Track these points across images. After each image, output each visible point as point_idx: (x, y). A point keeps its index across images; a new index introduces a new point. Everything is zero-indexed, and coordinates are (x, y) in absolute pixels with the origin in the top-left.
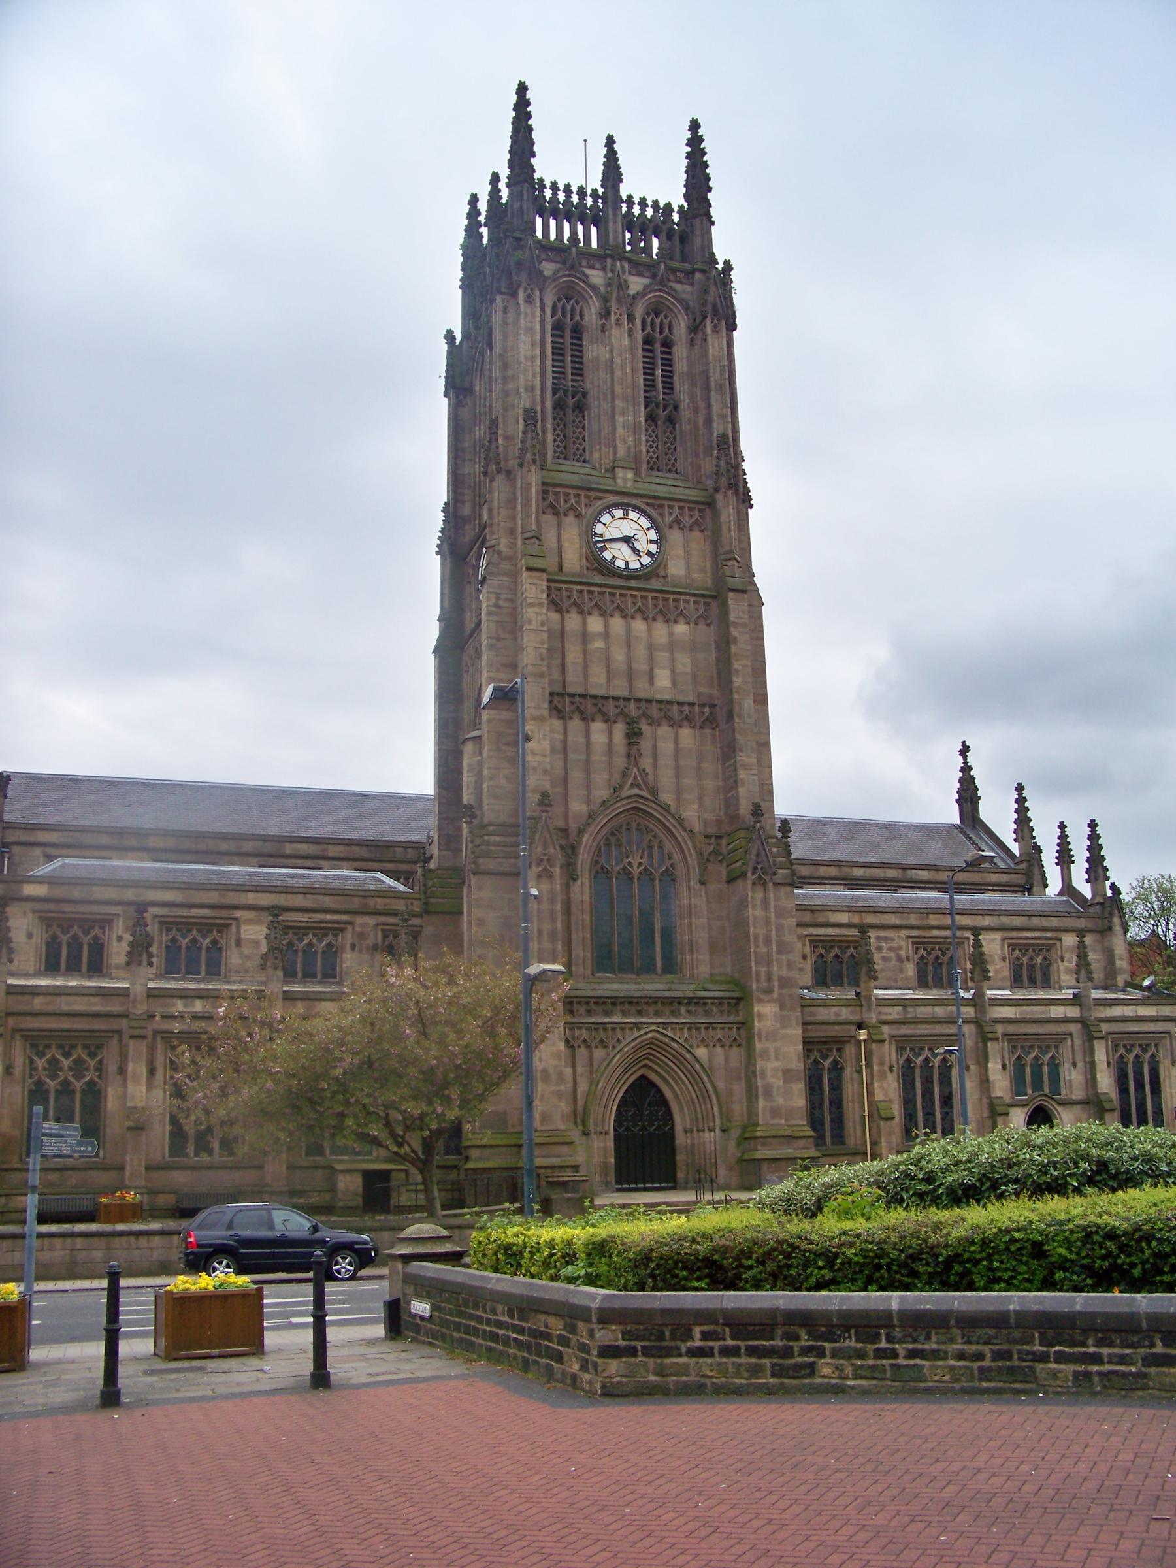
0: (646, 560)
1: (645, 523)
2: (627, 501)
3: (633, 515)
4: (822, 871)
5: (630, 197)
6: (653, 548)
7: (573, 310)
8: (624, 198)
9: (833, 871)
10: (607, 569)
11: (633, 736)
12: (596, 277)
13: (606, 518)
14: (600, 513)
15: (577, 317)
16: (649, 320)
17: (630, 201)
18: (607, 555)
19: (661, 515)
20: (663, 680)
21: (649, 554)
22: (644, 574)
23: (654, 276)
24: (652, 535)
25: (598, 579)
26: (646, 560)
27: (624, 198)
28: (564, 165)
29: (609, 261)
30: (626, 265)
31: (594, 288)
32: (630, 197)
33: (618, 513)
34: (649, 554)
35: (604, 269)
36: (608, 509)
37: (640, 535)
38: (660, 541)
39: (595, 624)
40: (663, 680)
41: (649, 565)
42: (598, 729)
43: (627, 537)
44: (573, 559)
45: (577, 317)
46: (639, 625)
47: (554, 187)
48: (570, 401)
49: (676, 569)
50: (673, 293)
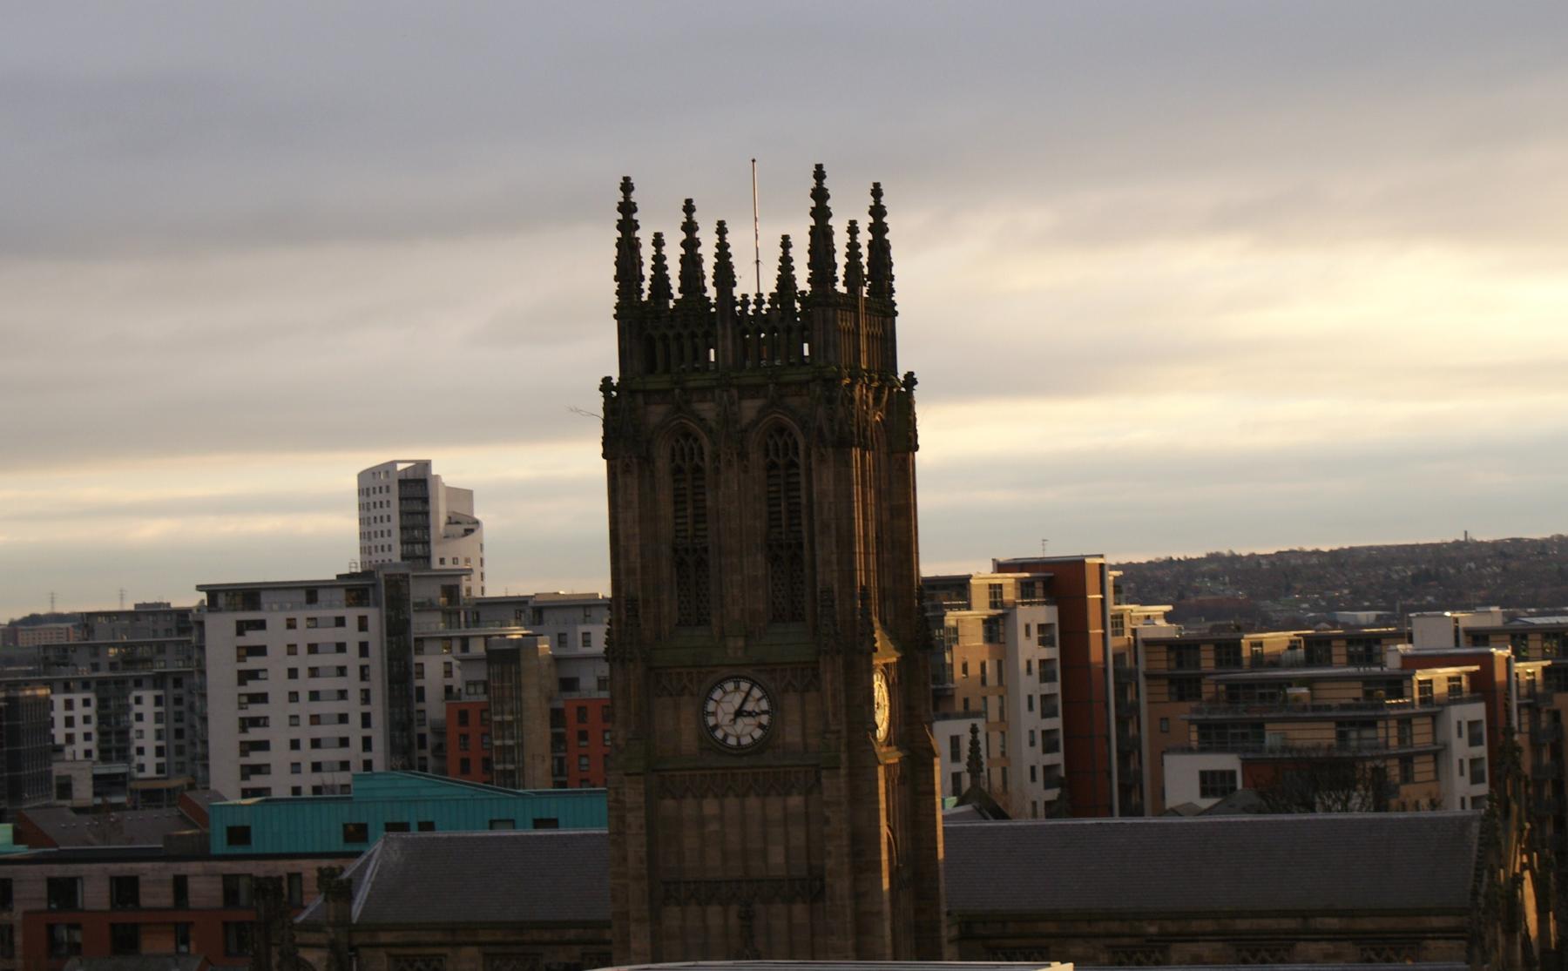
4: (1195, 925)
5: (745, 296)
8: (739, 299)
9: (1209, 925)
10: (721, 747)
11: (747, 917)
12: (707, 410)
13: (717, 695)
14: (712, 690)
15: (696, 459)
16: (771, 443)
17: (745, 301)
18: (719, 734)
20: (777, 856)
22: (758, 747)
26: (758, 733)
27: (739, 299)
29: (717, 392)
32: (745, 296)
34: (761, 726)
36: (719, 684)
38: (775, 709)
39: (710, 807)
40: (777, 856)
41: (761, 738)
42: (714, 913)
43: (736, 714)
44: (689, 739)
45: (696, 459)
46: (753, 802)
49: (792, 735)
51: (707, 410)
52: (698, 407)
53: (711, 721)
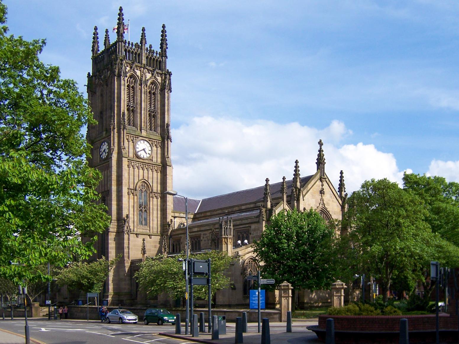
0: (148, 155)
1: (148, 145)
2: (144, 139)
3: (146, 142)
6: (150, 152)
7: (132, 81)
19: (152, 143)
21: (149, 154)
23: (153, 74)
24: (150, 149)
25: (138, 160)
26: (148, 155)
28: (132, 36)
30: (146, 70)
31: (138, 76)
33: (142, 141)
34: (149, 154)
35: (141, 71)
37: (147, 148)
43: (143, 148)
47: (129, 44)
48: (132, 110)
50: (157, 80)
51: (138, 73)
52: (135, 70)
53: (138, 150)
